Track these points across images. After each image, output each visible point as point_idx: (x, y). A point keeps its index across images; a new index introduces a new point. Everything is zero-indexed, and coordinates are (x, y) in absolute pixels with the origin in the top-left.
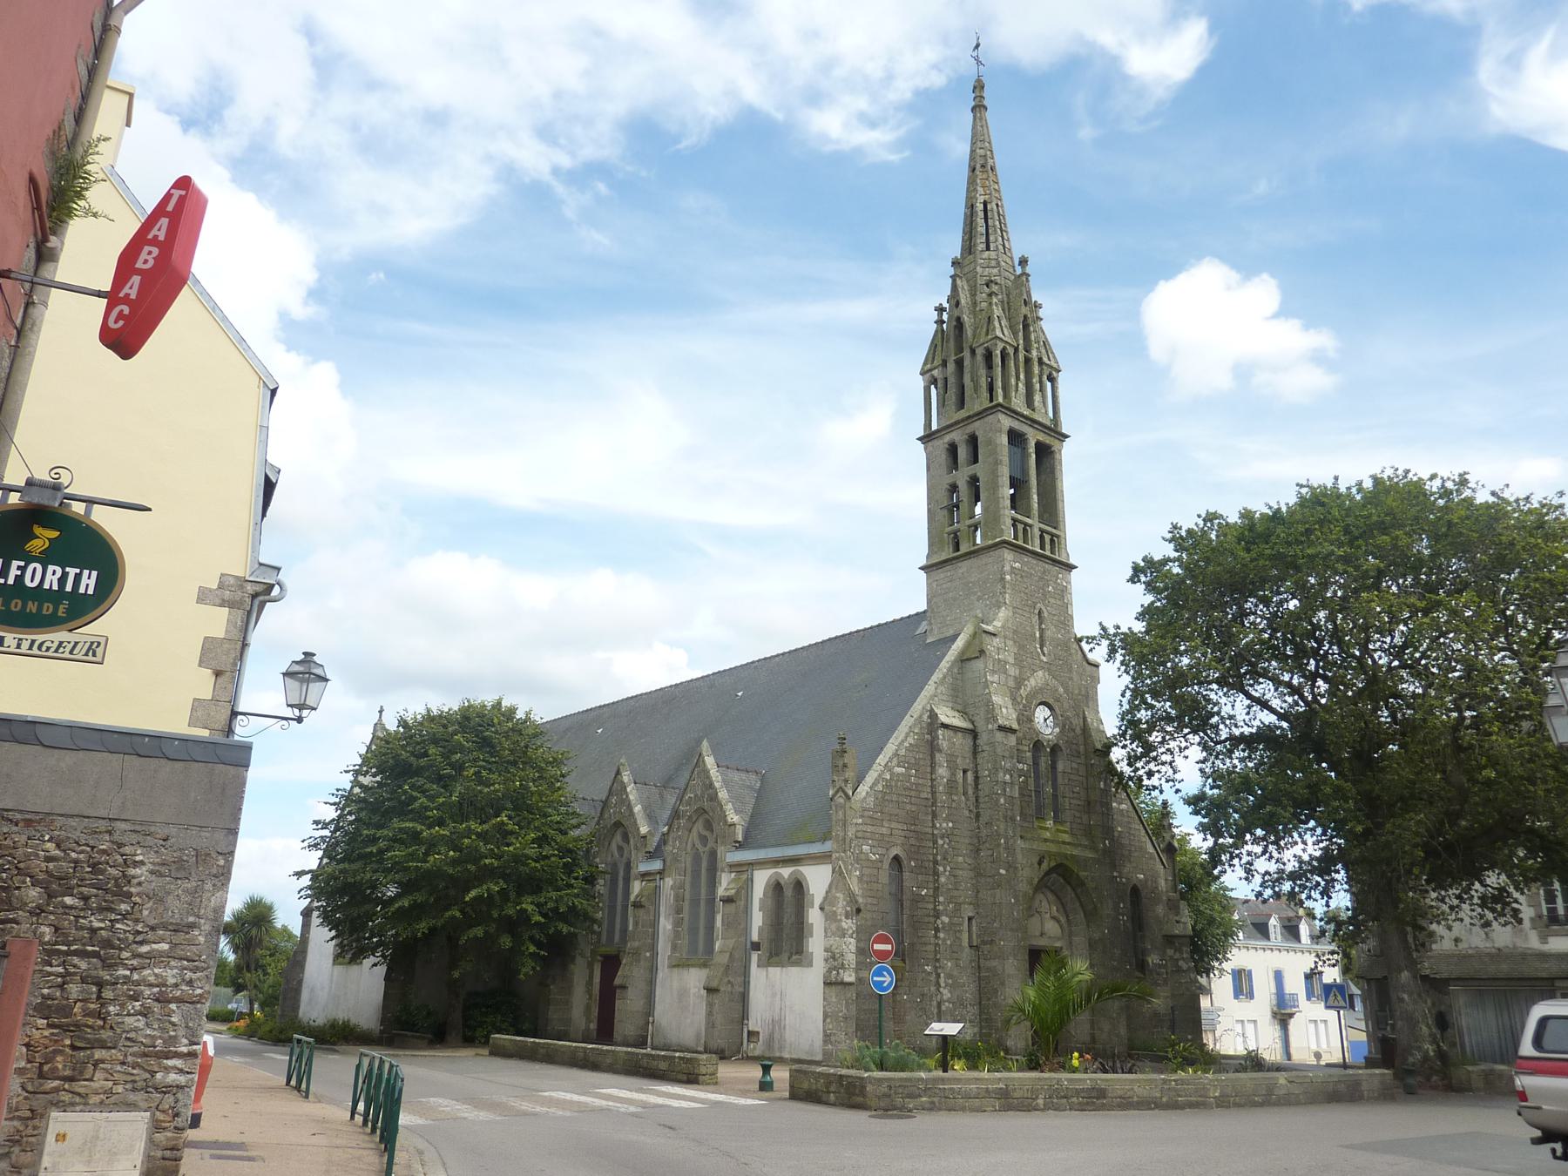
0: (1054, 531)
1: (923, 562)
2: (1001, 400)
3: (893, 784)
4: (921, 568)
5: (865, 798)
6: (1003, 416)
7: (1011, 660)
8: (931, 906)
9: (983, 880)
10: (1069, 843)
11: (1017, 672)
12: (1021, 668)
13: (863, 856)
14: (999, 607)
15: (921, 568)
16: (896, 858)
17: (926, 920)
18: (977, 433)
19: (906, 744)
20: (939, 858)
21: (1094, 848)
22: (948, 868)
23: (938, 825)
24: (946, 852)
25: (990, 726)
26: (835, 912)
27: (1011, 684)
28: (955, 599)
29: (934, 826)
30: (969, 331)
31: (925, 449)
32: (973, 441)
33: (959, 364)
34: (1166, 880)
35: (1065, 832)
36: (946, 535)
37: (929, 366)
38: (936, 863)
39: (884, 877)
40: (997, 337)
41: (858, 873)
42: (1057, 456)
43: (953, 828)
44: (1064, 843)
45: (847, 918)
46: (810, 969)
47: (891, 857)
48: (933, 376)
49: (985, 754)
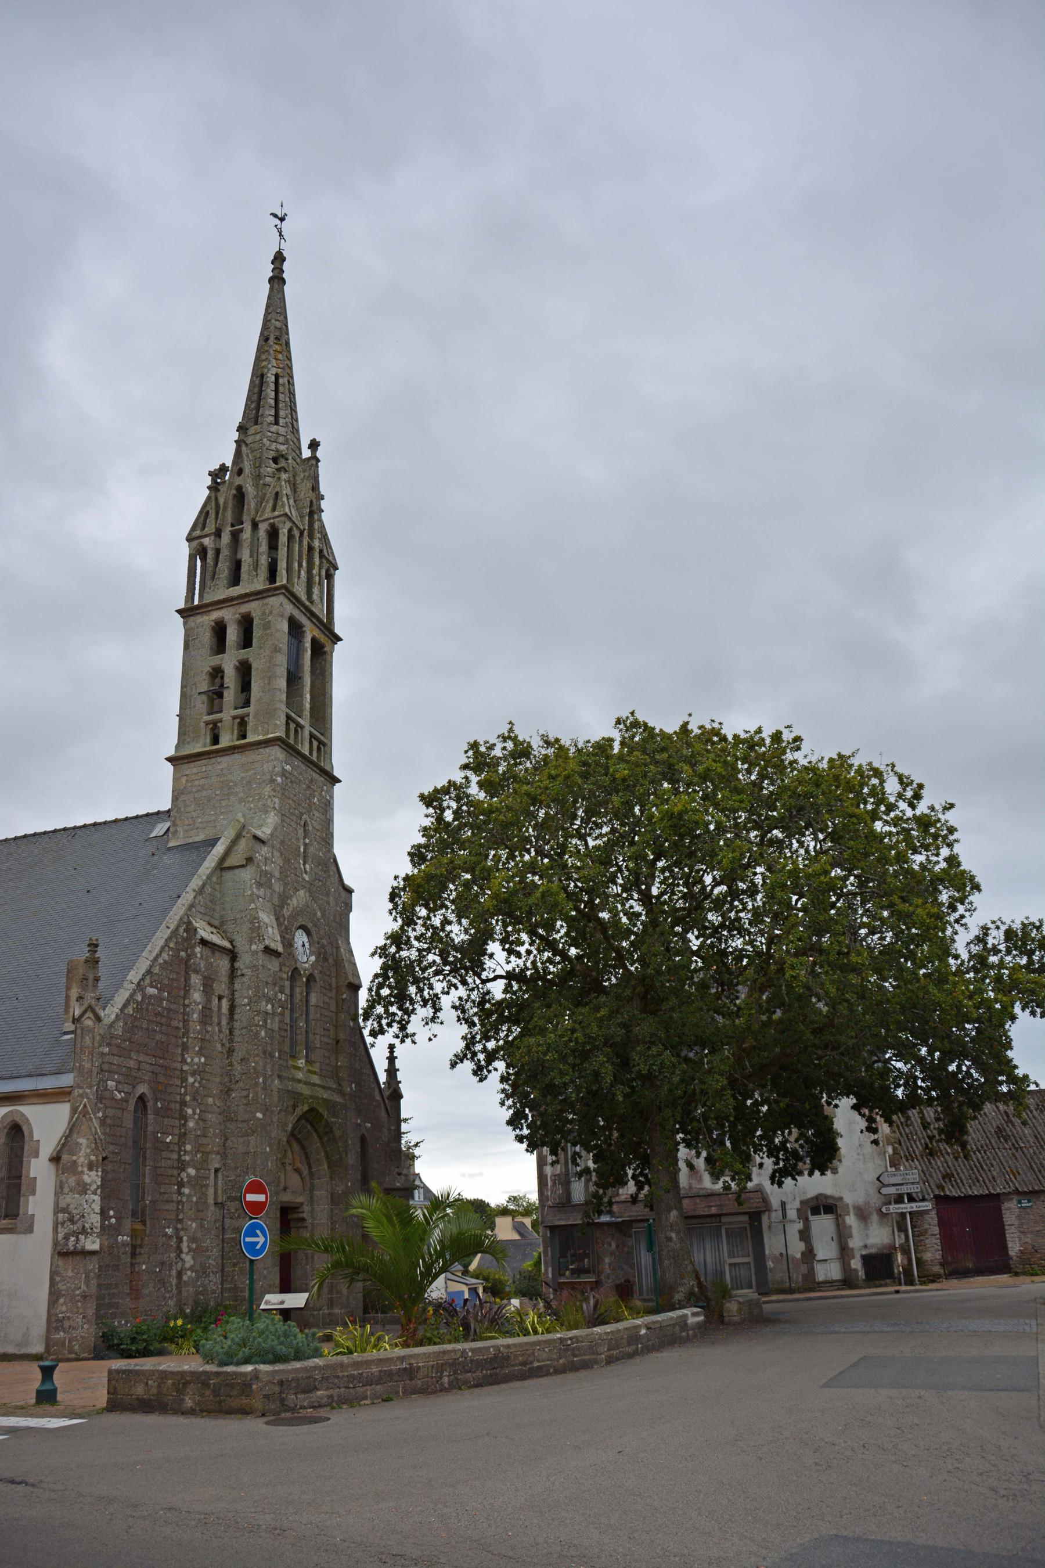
0: (322, 738)
1: (171, 752)
2: (285, 581)
4: (169, 759)
5: (113, 1022)
7: (277, 874)
8: (175, 1156)
9: (232, 1126)
10: (319, 1086)
11: (282, 889)
12: (286, 884)
13: (107, 1094)
14: (267, 812)
15: (169, 759)
16: (142, 1098)
17: (170, 1172)
18: (253, 614)
19: (161, 961)
20: (188, 1098)
21: (341, 1092)
22: (198, 1111)
23: (189, 1060)
24: (197, 1091)
25: (254, 947)
26: (75, 1162)
27: (276, 901)
28: (209, 799)
29: (184, 1061)
30: (251, 503)
31: (185, 624)
32: (247, 624)
33: (235, 536)
34: (389, 1129)
35: (314, 1073)
36: (202, 725)
37: (198, 533)
38: (183, 1104)
40: (286, 515)
42: (328, 657)
43: (205, 1064)
44: (314, 1085)
45: (90, 1169)
46: (28, 1236)
47: (137, 1096)
48: (202, 545)
49: (245, 979)
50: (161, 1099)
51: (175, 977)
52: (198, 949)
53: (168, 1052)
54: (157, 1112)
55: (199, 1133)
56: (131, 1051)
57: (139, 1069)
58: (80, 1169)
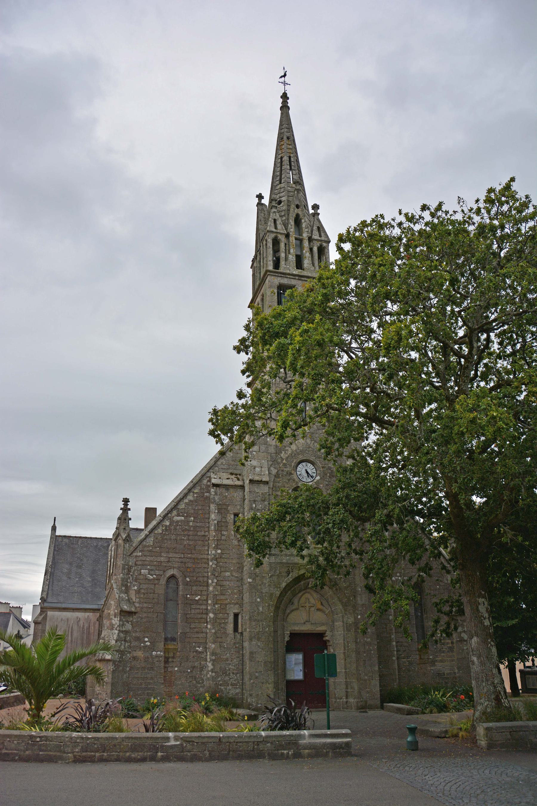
3: (173, 527)
6: (273, 277)
13: (141, 577)
16: (173, 576)
26: (109, 613)
39: (160, 590)
41: (136, 588)
43: (222, 553)
45: (115, 617)
50: (189, 576)
51: (200, 508)
52: (212, 490)
53: (195, 550)
54: (187, 584)
55: (217, 593)
56: (161, 552)
57: (169, 562)
58: (111, 617)
